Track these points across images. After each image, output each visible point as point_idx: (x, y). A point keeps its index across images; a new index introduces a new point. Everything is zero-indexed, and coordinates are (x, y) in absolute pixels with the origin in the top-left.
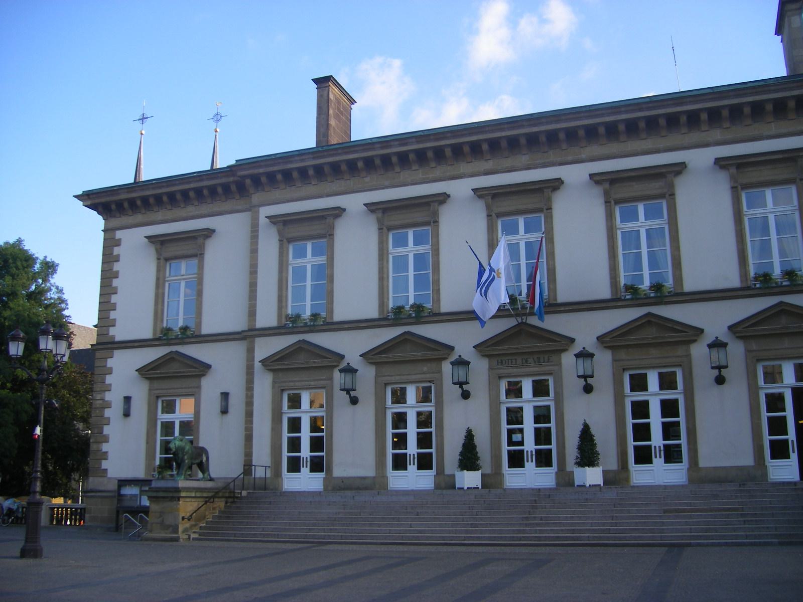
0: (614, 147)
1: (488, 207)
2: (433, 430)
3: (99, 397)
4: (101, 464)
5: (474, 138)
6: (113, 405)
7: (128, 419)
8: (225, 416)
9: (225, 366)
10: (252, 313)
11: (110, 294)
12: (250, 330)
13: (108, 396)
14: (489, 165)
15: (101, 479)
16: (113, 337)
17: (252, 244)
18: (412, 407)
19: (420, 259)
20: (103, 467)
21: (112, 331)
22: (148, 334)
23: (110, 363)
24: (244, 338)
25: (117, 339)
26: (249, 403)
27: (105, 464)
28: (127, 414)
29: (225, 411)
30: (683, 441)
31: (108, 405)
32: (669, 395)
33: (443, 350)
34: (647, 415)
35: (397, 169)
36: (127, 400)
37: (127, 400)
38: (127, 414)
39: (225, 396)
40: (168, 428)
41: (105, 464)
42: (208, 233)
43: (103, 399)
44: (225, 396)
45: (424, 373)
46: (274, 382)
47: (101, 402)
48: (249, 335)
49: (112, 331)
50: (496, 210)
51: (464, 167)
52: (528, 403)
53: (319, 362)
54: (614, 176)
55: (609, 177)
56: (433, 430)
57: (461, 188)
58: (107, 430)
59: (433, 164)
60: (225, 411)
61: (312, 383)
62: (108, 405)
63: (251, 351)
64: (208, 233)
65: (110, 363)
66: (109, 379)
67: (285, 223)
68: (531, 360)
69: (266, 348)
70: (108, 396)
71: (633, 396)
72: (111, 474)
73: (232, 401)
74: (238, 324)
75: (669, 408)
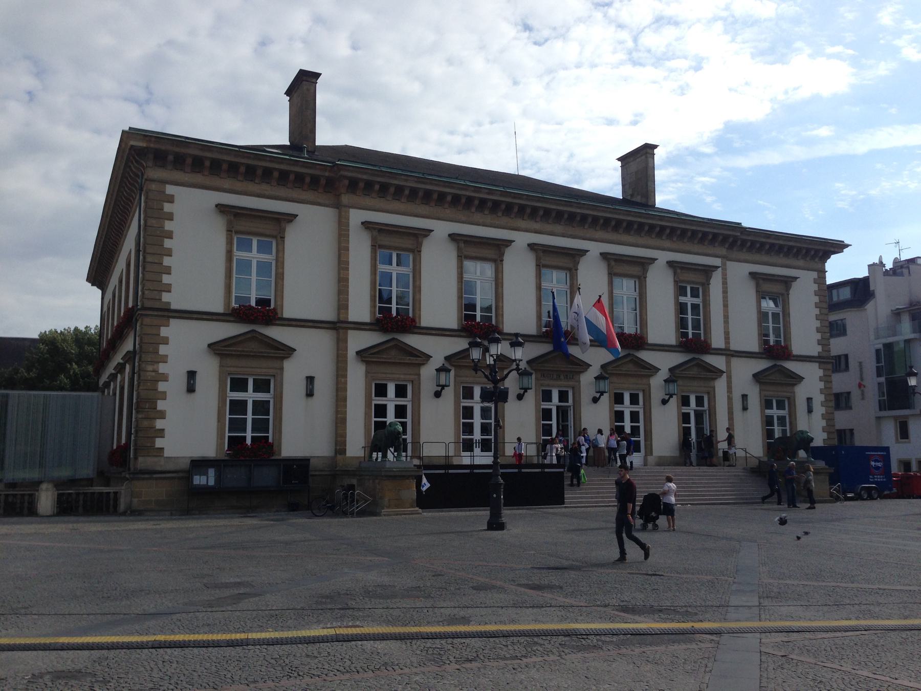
2: (374, 419)
3: (150, 368)
4: (154, 443)
6: (170, 378)
7: (193, 395)
8: (310, 399)
9: (310, 354)
11: (162, 255)
13: (162, 368)
15: (156, 459)
16: (169, 303)
17: (339, 242)
20: (157, 446)
21: (165, 297)
22: (219, 308)
23: (164, 332)
25: (174, 306)
27: (159, 443)
28: (191, 389)
29: (310, 394)
30: (642, 439)
31: (165, 378)
32: (401, 402)
35: (446, 206)
36: (192, 375)
37: (192, 375)
38: (191, 389)
39: (310, 380)
40: (238, 407)
41: (159, 443)
42: (291, 218)
43: (156, 371)
44: (310, 380)
46: (367, 372)
47: (153, 374)
48: (339, 326)
49: (165, 297)
50: (543, 262)
53: (408, 359)
56: (374, 419)
58: (161, 405)
59: (486, 212)
60: (310, 394)
61: (402, 376)
62: (165, 378)
64: (291, 218)
65: (164, 332)
66: (163, 350)
67: (380, 231)
68: (562, 377)
69: (358, 341)
70: (162, 368)
72: (167, 454)
75: (634, 416)
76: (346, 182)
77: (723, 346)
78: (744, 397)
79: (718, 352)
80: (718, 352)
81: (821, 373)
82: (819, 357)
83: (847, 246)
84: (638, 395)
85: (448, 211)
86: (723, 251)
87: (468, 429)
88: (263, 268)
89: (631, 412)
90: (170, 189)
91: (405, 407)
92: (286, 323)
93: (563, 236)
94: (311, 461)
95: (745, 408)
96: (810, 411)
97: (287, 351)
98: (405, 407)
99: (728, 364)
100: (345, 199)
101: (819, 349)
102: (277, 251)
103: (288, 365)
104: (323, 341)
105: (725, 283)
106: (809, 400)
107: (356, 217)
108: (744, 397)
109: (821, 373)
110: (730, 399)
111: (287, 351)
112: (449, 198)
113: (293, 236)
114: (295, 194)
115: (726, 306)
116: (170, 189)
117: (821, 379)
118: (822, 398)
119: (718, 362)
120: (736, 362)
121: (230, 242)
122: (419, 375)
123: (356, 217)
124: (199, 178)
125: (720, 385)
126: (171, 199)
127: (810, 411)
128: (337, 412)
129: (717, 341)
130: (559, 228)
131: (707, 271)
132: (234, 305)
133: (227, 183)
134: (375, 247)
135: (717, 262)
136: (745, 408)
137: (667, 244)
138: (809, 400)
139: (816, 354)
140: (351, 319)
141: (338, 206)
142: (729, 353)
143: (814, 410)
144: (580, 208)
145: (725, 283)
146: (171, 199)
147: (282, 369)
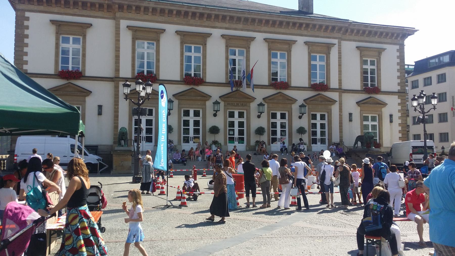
0: (272, 29)
1: (226, 43)
5: (225, 14)
8: (100, 116)
9: (101, 94)
10: (117, 70)
12: (116, 78)
14: (227, 25)
16: (26, 70)
17: (116, 37)
18: (191, 119)
19: (197, 59)
22: (52, 72)
24: (113, 81)
25: (29, 72)
26: (116, 111)
29: (100, 113)
33: (207, 97)
34: (276, 127)
39: (100, 107)
44: (100, 107)
45: (199, 105)
48: (115, 79)
51: (217, 24)
52: (236, 120)
54: (273, 40)
55: (272, 40)
57: (217, 33)
60: (100, 113)
63: (116, 88)
71: (244, 120)
73: (104, 110)
74: (109, 72)
76: (117, 6)
77: (337, 86)
78: (350, 115)
79: (334, 90)
80: (334, 90)
81: (399, 101)
82: (398, 92)
83: (416, 31)
84: (325, 115)
85: (175, 19)
86: (339, 35)
87: (187, 131)
88: (76, 52)
89: (321, 124)
90: (27, 14)
91: (151, 120)
92: (87, 78)
93: (242, 30)
94: (99, 147)
95: (351, 120)
96: (391, 121)
97: (88, 93)
98: (151, 120)
99: (340, 96)
100: (118, 14)
101: (399, 88)
102: (83, 42)
103: (88, 99)
104: (108, 87)
105: (340, 53)
106: (391, 116)
107: (124, 23)
108: (350, 115)
109: (399, 101)
110: (341, 116)
111: (88, 93)
112: (175, 12)
113: (91, 34)
114: (92, 13)
115: (340, 65)
116: (27, 14)
117: (399, 104)
118: (400, 115)
119: (334, 96)
120: (345, 95)
121: (57, 39)
122: (205, 105)
123: (124, 23)
124: (41, 8)
125: (335, 109)
126: (28, 19)
127: (391, 121)
128: (115, 123)
129: (334, 84)
130: (240, 26)
131: (329, 47)
132: (60, 70)
133: (56, 9)
134: (134, 39)
135: (336, 41)
136: (351, 120)
137: (305, 32)
138: (391, 116)
139: (397, 91)
140: (121, 76)
141: (114, 18)
142: (341, 90)
143: (394, 121)
144: (249, 15)
145: (340, 53)
146: (28, 19)
147: (85, 101)
